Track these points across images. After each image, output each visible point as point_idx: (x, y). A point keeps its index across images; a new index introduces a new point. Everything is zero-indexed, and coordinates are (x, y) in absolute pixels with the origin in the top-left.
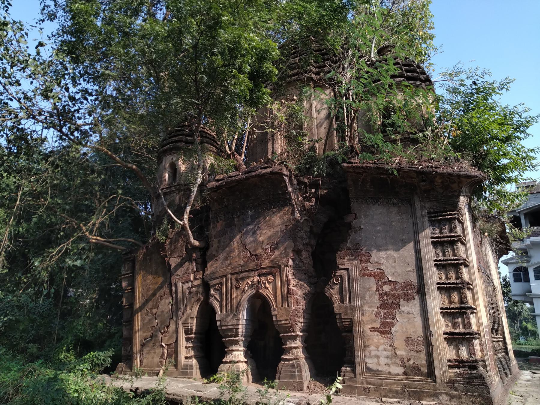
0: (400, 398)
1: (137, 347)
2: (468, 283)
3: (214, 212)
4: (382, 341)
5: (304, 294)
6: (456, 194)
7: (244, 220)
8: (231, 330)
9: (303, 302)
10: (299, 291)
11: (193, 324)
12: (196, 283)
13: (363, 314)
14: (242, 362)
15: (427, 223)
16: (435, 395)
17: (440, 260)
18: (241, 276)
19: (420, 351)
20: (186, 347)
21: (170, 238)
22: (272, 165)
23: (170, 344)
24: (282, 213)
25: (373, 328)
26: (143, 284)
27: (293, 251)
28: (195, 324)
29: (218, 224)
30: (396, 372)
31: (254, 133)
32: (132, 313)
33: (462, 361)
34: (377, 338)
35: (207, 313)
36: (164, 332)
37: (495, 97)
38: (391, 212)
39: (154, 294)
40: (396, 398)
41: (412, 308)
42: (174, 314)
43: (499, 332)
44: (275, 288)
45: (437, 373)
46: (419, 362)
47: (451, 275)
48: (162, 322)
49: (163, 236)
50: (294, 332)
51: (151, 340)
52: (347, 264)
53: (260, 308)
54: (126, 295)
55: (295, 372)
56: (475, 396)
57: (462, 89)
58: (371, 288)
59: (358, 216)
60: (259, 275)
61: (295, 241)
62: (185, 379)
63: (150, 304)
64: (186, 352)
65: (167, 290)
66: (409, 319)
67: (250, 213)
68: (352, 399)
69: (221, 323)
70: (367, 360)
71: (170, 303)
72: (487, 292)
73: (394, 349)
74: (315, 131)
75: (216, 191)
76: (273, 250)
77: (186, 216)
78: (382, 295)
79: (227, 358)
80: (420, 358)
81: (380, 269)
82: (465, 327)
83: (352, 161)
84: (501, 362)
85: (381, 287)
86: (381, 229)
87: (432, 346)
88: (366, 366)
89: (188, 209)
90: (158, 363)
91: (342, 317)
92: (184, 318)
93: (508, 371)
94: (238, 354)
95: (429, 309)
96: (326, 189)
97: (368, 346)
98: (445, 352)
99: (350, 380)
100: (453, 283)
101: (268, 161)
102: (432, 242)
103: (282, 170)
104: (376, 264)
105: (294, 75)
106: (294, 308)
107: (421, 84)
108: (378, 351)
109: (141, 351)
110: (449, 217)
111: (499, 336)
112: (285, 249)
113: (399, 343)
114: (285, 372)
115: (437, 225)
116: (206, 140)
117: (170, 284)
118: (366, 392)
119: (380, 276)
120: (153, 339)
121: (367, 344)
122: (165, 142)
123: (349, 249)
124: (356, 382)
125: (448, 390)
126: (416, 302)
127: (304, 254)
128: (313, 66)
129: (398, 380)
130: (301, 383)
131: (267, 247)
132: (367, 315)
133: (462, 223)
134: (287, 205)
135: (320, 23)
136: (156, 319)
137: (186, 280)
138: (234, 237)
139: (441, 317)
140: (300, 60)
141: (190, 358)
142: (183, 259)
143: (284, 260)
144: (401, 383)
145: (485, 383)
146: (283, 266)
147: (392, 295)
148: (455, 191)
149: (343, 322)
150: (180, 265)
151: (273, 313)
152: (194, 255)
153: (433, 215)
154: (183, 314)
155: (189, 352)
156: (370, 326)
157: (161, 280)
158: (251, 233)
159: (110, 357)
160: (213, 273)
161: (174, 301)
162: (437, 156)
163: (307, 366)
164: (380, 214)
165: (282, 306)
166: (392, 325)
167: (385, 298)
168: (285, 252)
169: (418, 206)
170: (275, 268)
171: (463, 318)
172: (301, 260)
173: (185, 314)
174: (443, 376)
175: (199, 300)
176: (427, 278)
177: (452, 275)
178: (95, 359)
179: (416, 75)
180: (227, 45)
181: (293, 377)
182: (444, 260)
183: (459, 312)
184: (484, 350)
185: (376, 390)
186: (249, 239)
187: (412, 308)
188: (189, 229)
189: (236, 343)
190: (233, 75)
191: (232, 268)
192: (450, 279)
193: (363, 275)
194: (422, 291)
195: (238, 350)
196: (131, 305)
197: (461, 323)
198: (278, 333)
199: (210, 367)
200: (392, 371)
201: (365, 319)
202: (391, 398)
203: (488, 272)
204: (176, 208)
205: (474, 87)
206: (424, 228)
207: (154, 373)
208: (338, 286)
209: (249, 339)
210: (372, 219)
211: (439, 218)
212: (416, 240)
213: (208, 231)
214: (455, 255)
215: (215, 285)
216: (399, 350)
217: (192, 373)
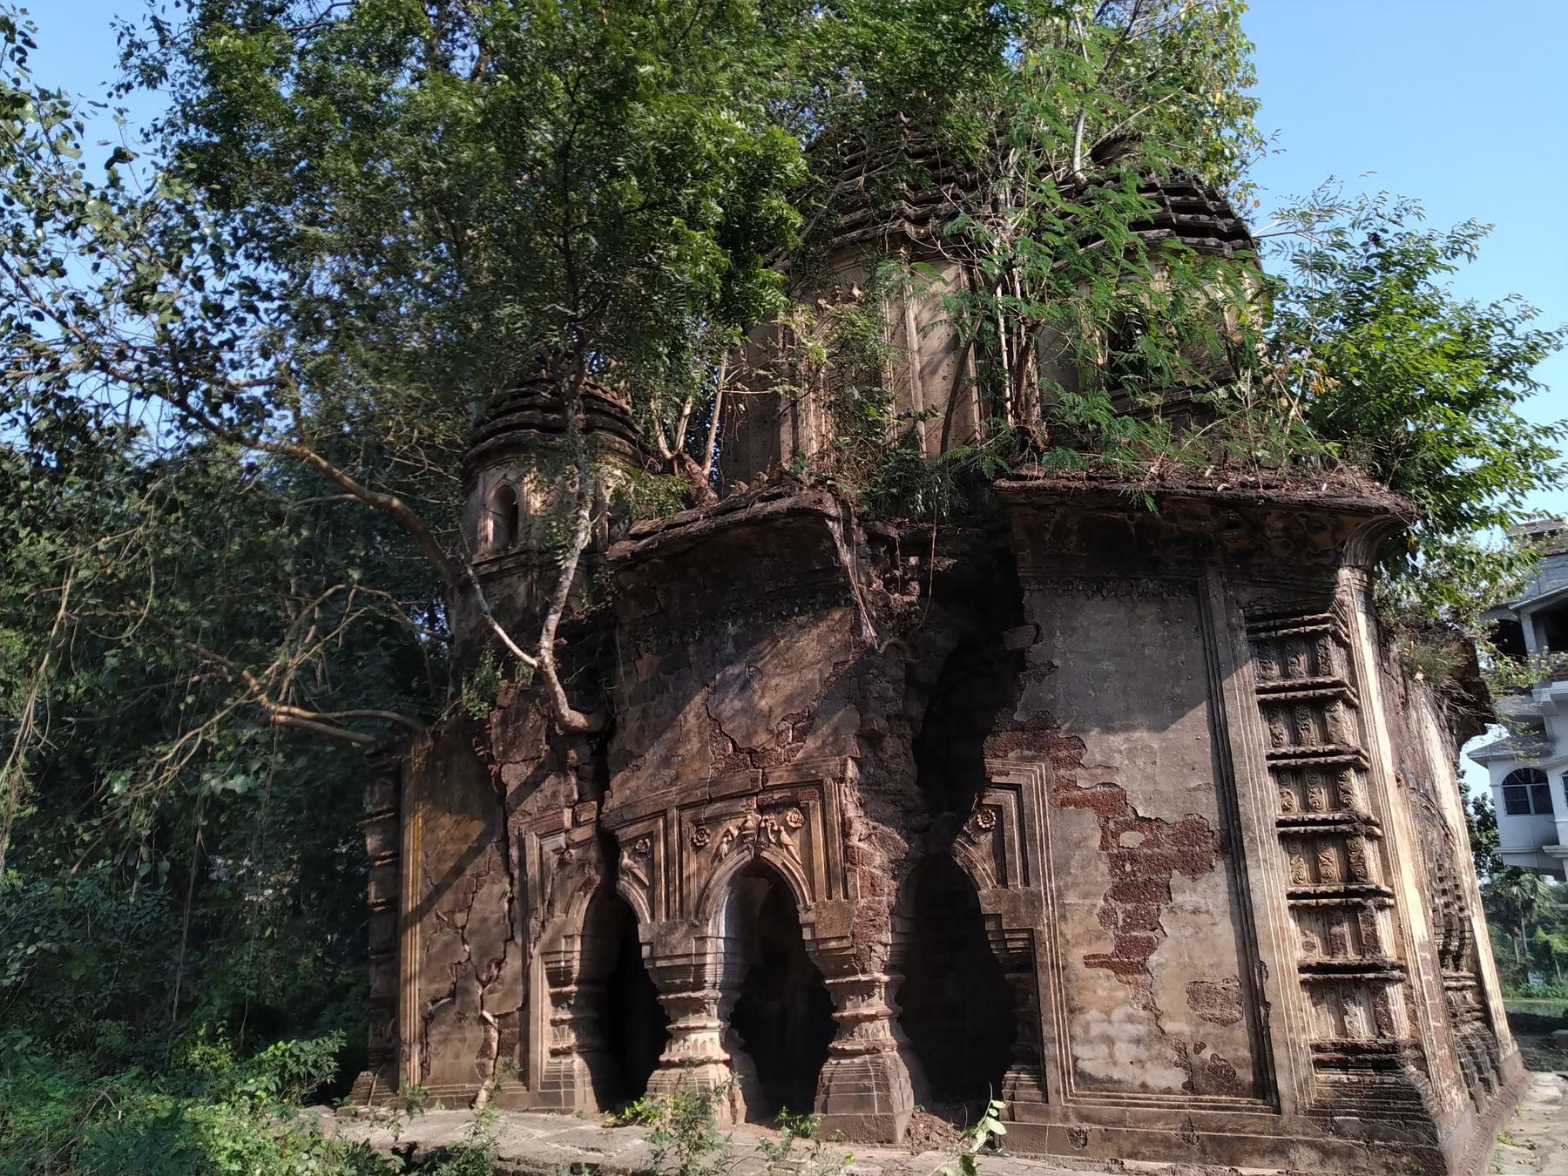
0: (1176, 1159)
1: (411, 1024)
2: (1368, 822)
3: (627, 628)
4: (1120, 994)
5: (892, 862)
6: (1327, 561)
7: (715, 650)
9: (889, 885)
10: (876, 853)
11: (573, 955)
12: (579, 835)
13: (1063, 917)
14: (716, 1062)
15: (1244, 648)
16: (1279, 1150)
17: (1285, 756)
18: (708, 812)
19: (1233, 1021)
20: (554, 1023)
21: (501, 708)
22: (793, 488)
23: (508, 1014)
24: (823, 627)
25: (1094, 956)
26: (427, 840)
27: (859, 736)
28: (577, 956)
29: (639, 664)
30: (1163, 1084)
31: (738, 398)
32: (396, 926)
33: (1355, 1049)
35: (612, 923)
36: (490, 980)
37: (1436, 278)
39: (458, 871)
40: (1165, 1160)
41: (1204, 895)
43: (1463, 962)
44: (807, 846)
46: (1228, 1054)
47: (1317, 796)
48: (483, 951)
49: (483, 700)
50: (864, 971)
51: (452, 1003)
52: (1015, 772)
53: (765, 903)
54: (378, 874)
55: (869, 1089)
56: (1394, 1151)
57: (1340, 256)
58: (1085, 839)
59: (1044, 631)
60: (762, 810)
61: (862, 707)
62: (550, 1116)
63: (447, 900)
64: (552, 1036)
65: (497, 858)
66: (1198, 929)
67: (731, 629)
68: (1038, 1163)
69: (652, 950)
70: (1079, 1051)
71: (505, 894)
72: (1424, 844)
73: (1157, 1017)
74: (917, 388)
75: (631, 568)
76: (801, 736)
77: (547, 643)
78: (1117, 861)
79: (673, 1053)
80: (1232, 1041)
82: (1361, 951)
83: (1024, 472)
84: (1469, 1047)
85: (1116, 835)
87: (1267, 1005)
88: (1075, 1066)
89: (553, 620)
90: (472, 1071)
91: (1005, 927)
92: (545, 937)
93: (1491, 1075)
94: (704, 1040)
96: (950, 555)
98: (1305, 1024)
99: (1030, 1109)
100: (1325, 822)
101: (781, 478)
102: (1262, 703)
103: (820, 501)
104: (1099, 771)
105: (852, 227)
106: (863, 902)
107: (1219, 246)
108: (1110, 1022)
109: (424, 1035)
110: (1309, 628)
111: (1465, 973)
112: (836, 731)
113: (1171, 998)
114: (841, 1088)
115: (1274, 653)
116: (600, 420)
117: (505, 838)
118: (1078, 1141)
119: (1111, 804)
120: (458, 1002)
121: (1077, 1002)
122: (483, 429)
123: (1022, 728)
124: (1048, 1113)
125: (1314, 1133)
126: (1219, 878)
127: (891, 745)
128: (908, 200)
129: (1171, 1107)
130: (889, 1120)
131: (783, 726)
132: (1076, 918)
133: (1347, 646)
135: (924, 76)
136: (464, 941)
137: (552, 827)
138: (687, 699)
139: (1292, 922)
140: (870, 182)
141: (566, 1052)
143: (834, 764)
144: (1177, 1114)
145: (1421, 1111)
146: (829, 781)
147: (1149, 858)
148: (1325, 553)
150: (531, 785)
151: (804, 917)
152: (572, 753)
154: (543, 925)
155: (562, 1036)
156: (1085, 951)
157: (477, 828)
158: (735, 688)
159: (333, 1054)
160: (625, 805)
161: (517, 888)
162: (1270, 454)
163: (905, 1072)
164: (1107, 624)
165: (830, 897)
166: (1150, 946)
167: (1128, 868)
168: (836, 740)
169: (1217, 598)
170: (807, 789)
171: (1354, 922)
172: (882, 765)
173: (549, 927)
174: (1301, 1091)
175: (588, 883)
176: (1248, 808)
177: (1322, 796)
178: (290, 1063)
179: (1204, 218)
180: (654, 148)
181: (863, 1102)
182: (1295, 756)
183: (1344, 905)
184: (1420, 1014)
185: (1107, 1137)
186: (731, 705)
187: (1204, 895)
188: (555, 679)
189: (698, 1006)
190: (674, 233)
191: (682, 791)
192: (1315, 810)
193: (1063, 804)
195: (704, 1028)
196: (394, 903)
197: (1348, 937)
198: (820, 977)
199: (622, 1076)
200: (1151, 1082)
201: (1070, 929)
202: (1150, 1159)
203: (1428, 785)
204: (517, 618)
205: (1373, 249)
206: (1236, 663)
207: (462, 1099)
208: (990, 835)
209: (737, 996)
210: (1086, 638)
211: (1280, 633)
212: (1215, 700)
213: (610, 683)
214: (1327, 739)
215: (635, 840)
216: (1172, 1019)
217: (570, 1098)
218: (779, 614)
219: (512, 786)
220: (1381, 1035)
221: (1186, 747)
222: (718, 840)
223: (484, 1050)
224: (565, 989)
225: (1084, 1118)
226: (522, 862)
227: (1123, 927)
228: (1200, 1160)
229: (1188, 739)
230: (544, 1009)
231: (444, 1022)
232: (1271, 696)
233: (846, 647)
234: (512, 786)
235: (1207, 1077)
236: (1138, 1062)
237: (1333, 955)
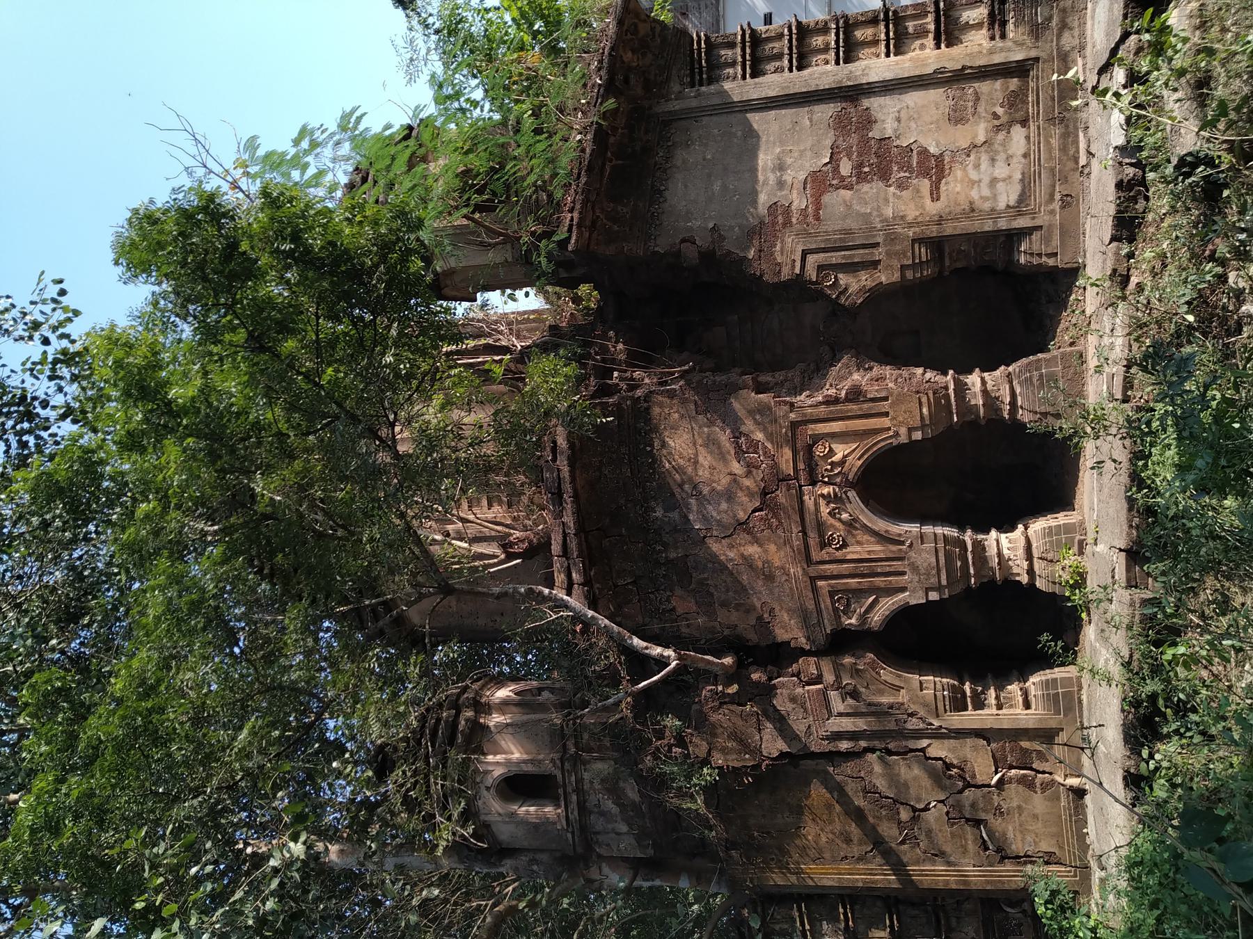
0: (1076, 129)
4: (959, 173)
6: (658, 29)
7: (675, 530)
8: (948, 555)
9: (877, 370)
10: (849, 376)
13: (903, 217)
20: (1000, 707)
29: (680, 611)
30: (1023, 141)
33: (991, 15)
38: (684, 162)
39: (858, 816)
40: (1077, 136)
41: (888, 114)
42: (912, 744)
46: (999, 96)
50: (946, 388)
51: (984, 822)
53: (894, 482)
54: (861, 928)
58: (845, 201)
59: (687, 235)
62: (1084, 697)
63: (888, 831)
65: (849, 767)
66: (910, 118)
67: (659, 513)
69: (932, 589)
70: (1002, 205)
78: (861, 177)
80: (990, 93)
81: (805, 183)
82: (925, 14)
85: (843, 179)
87: (964, 68)
91: (910, 262)
92: (922, 713)
94: (1005, 545)
95: (889, 76)
97: (971, 203)
98: (976, 46)
99: (1047, 240)
102: (753, 76)
106: (891, 385)
108: (980, 181)
110: (703, 45)
113: (961, 137)
118: (1068, 201)
119: (819, 183)
120: (983, 816)
124: (1050, 225)
125: (1051, 35)
126: (874, 104)
129: (1039, 135)
134: (648, 409)
137: (820, 709)
138: (714, 558)
141: (1026, 694)
144: (1044, 129)
147: (860, 155)
148: (653, 29)
150: (781, 723)
151: (903, 439)
152: (755, 676)
154: (912, 715)
155: (1010, 699)
156: (928, 201)
157: (818, 793)
161: (877, 744)
164: (686, 186)
166: (924, 152)
167: (866, 169)
169: (675, 106)
171: (905, 18)
176: (825, 83)
177: (818, 41)
187: (888, 114)
189: (979, 547)
192: (828, 44)
193: (818, 219)
194: (852, 94)
200: (1022, 151)
207: (1076, 808)
208: (840, 276)
210: (692, 204)
216: (976, 136)
217: (1067, 681)
218: (651, 465)
219: (782, 746)
221: (781, 128)
222: (838, 524)
223: (1028, 784)
225: (1051, 198)
226: (853, 736)
229: (775, 127)
231: (1004, 834)
233: (684, 402)
234: (782, 746)
235: (1017, 111)
237: (928, 32)
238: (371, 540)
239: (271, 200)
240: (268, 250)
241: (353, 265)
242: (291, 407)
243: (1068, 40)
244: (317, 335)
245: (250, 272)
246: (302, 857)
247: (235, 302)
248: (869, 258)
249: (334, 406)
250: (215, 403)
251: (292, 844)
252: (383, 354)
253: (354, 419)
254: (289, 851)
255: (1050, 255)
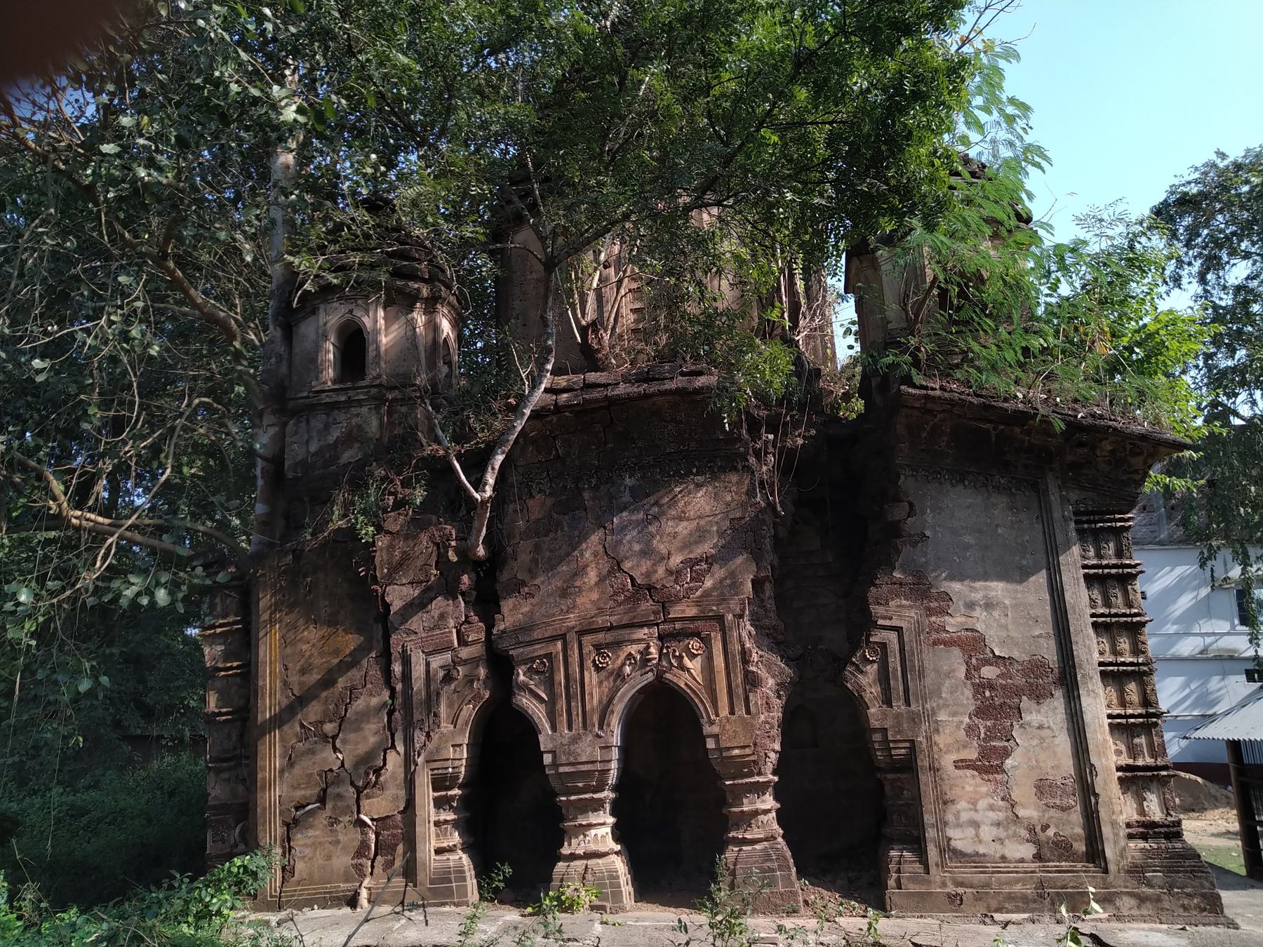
0: (1032, 911)
3: (521, 470)
4: (984, 789)
5: (778, 684)
6: (1137, 477)
7: (611, 498)
8: (588, 774)
9: (777, 703)
10: (771, 674)
13: (937, 731)
19: (1070, 808)
20: (437, 824)
21: (388, 532)
25: (962, 761)
29: (530, 503)
30: (1018, 855)
33: (1154, 825)
34: (972, 782)
38: (994, 505)
39: (328, 681)
40: (1024, 912)
41: (1048, 715)
45: (1109, 853)
46: (1067, 832)
50: (760, 774)
53: (663, 721)
54: (218, 684)
58: (953, 671)
62: (447, 909)
63: (313, 711)
65: (376, 673)
66: (1042, 739)
67: (628, 481)
69: (554, 757)
70: (951, 833)
78: (979, 688)
79: (574, 846)
80: (1069, 822)
81: (972, 630)
82: (1154, 755)
85: (977, 669)
86: (972, 541)
87: (1096, 795)
90: (346, 873)
91: (890, 738)
92: (430, 746)
94: (600, 832)
95: (1088, 717)
97: (953, 801)
98: (1120, 809)
99: (914, 879)
102: (1086, 576)
106: (762, 717)
108: (976, 811)
110: (1119, 524)
113: (1023, 792)
118: (955, 901)
119: (973, 644)
120: (329, 806)
124: (929, 882)
125: (1132, 886)
126: (1058, 702)
129: (1026, 872)
132: (947, 731)
134: (736, 469)
138: (584, 537)
141: (450, 850)
142: (428, 589)
144: (1032, 878)
147: (1003, 687)
148: (1136, 472)
149: (890, 749)
150: (419, 605)
151: (707, 729)
152: (465, 578)
153: (1084, 519)
154: (428, 735)
156: (955, 757)
157: (351, 641)
160: (525, 628)
161: (399, 700)
164: (968, 507)
166: (1006, 753)
167: (987, 694)
169: (1054, 497)
171: (1149, 735)
173: (435, 737)
176: (1079, 651)
177: (1124, 644)
185: (978, 898)
187: (1048, 715)
189: (597, 806)
192: (1121, 654)
193: (935, 643)
196: (244, 712)
198: (720, 778)
200: (1008, 854)
202: (1013, 912)
207: (338, 898)
208: (875, 666)
210: (950, 514)
216: (1024, 807)
217: (463, 891)
218: (677, 473)
220: (1168, 814)
222: (619, 662)
223: (361, 851)
224: (450, 793)
225: (961, 884)
226: (407, 677)
227: (984, 739)
228: (1049, 910)
230: (427, 811)
231: (311, 827)
232: (1092, 571)
233: (743, 506)
234: (396, 605)
236: (1001, 841)
238: (601, 184)
239: (957, 68)
240: (904, 68)
241: (888, 158)
242: (738, 98)
243: (1126, 904)
244: (812, 123)
245: (881, 48)
246: (282, 118)
247: (847, 35)
248: (894, 696)
249: (739, 142)
250: (740, 19)
251: (294, 107)
252: (794, 190)
253: (727, 160)
254: (287, 105)
255: (898, 881)
